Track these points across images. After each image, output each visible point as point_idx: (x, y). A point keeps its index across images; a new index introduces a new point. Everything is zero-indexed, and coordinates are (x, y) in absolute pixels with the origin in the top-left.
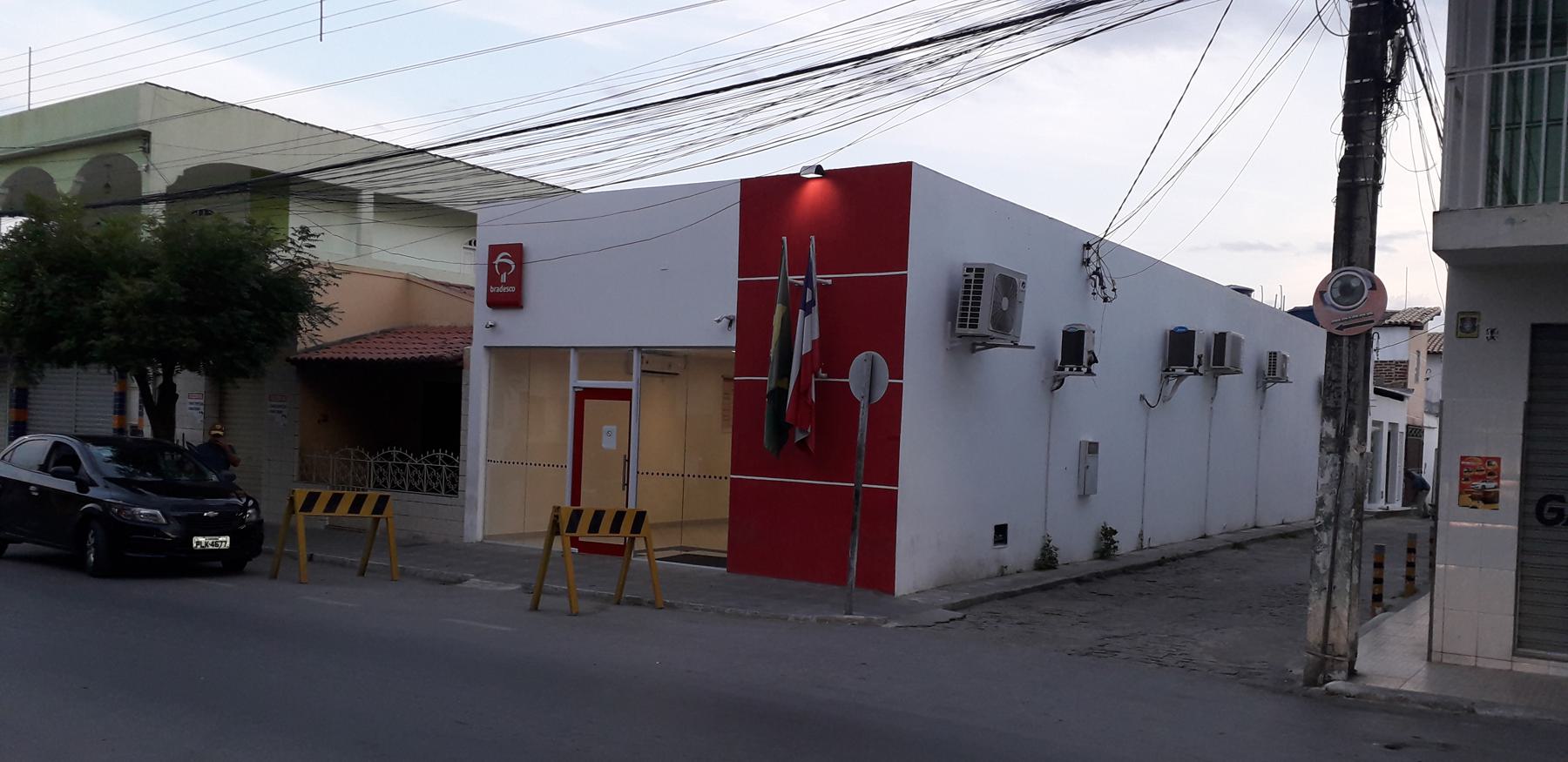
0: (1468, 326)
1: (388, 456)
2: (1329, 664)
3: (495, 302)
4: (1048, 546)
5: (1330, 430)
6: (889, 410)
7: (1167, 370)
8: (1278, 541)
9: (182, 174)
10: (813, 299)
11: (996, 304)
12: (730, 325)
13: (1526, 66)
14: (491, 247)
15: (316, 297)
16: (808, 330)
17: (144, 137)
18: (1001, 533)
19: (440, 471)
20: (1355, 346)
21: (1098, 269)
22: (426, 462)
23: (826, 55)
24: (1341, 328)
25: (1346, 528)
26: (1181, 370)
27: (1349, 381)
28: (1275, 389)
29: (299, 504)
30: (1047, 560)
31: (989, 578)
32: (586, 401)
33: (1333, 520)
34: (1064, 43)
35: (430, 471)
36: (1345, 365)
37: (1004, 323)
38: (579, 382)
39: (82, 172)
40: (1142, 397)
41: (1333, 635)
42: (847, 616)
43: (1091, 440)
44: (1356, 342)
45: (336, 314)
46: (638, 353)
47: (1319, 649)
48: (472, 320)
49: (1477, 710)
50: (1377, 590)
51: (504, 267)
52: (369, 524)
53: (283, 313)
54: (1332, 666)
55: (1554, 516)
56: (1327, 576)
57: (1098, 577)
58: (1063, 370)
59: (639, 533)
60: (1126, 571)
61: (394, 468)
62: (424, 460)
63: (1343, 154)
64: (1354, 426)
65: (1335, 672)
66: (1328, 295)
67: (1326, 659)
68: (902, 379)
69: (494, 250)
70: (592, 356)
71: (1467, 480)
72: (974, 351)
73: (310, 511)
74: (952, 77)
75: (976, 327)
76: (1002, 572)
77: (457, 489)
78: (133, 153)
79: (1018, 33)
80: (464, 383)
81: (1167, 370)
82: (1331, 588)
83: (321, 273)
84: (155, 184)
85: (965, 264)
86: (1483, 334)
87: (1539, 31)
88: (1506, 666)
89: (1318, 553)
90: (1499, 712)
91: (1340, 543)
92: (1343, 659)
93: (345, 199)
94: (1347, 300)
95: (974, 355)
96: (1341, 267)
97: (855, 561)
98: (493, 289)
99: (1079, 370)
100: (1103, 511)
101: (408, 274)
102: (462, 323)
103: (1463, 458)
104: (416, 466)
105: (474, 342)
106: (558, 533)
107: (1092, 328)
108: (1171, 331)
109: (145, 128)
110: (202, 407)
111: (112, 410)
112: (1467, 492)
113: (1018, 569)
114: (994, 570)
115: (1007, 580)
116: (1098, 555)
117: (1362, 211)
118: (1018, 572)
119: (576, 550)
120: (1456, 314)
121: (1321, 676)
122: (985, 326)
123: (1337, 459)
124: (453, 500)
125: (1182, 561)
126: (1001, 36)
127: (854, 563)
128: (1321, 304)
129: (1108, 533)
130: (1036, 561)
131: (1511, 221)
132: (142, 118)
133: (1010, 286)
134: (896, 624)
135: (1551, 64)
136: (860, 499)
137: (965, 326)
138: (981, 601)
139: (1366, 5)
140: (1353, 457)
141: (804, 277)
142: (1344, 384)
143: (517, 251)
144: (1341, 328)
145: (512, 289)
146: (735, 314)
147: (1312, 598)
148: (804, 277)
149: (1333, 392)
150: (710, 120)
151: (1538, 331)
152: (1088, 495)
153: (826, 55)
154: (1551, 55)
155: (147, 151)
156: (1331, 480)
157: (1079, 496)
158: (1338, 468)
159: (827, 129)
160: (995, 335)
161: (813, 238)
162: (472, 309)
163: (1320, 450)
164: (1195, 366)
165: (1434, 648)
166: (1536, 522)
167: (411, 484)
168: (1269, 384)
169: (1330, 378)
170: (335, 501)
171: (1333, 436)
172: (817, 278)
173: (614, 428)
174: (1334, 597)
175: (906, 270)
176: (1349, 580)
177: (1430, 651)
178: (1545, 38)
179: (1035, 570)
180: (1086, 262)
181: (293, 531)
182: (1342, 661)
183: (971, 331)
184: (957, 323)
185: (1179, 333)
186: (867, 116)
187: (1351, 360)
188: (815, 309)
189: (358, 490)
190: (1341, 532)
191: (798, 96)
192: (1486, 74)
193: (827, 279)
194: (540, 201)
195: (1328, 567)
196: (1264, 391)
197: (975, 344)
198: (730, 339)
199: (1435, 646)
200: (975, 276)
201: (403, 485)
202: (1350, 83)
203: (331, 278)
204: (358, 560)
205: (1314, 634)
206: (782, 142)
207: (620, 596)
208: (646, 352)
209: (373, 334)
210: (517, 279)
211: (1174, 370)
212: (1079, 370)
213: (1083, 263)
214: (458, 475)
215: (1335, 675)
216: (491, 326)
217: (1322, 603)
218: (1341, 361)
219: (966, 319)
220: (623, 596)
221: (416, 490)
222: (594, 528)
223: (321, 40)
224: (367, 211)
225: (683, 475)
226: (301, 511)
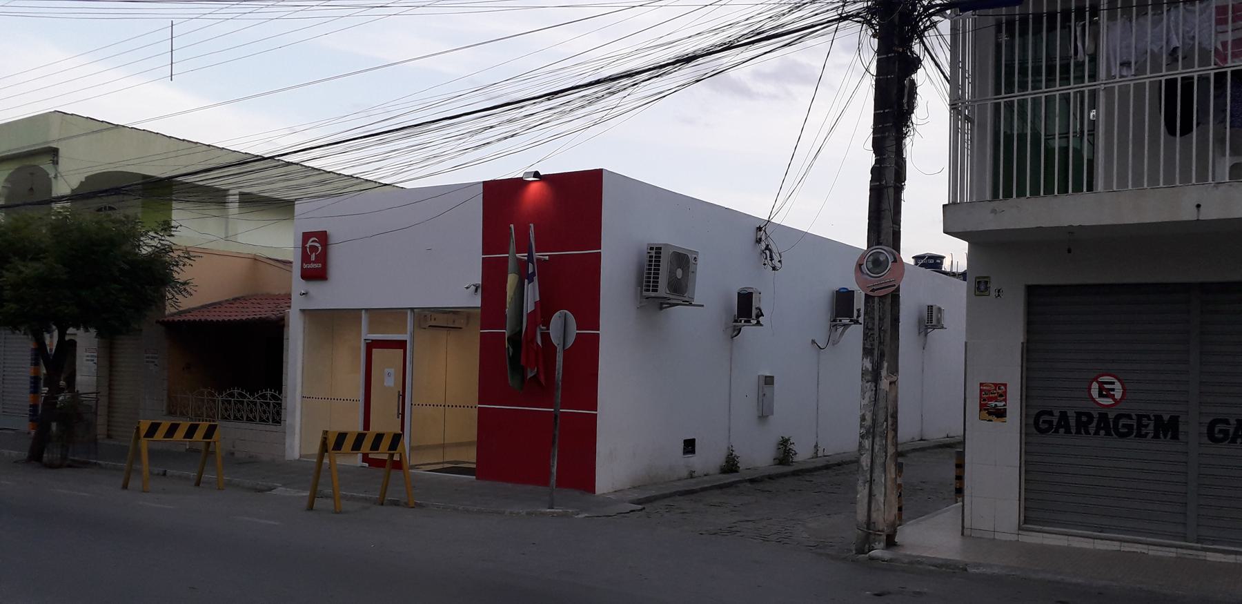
0: (982, 287)
1: (232, 395)
2: (872, 537)
3: (307, 275)
4: (732, 454)
5: (869, 366)
6: (587, 351)
7: (834, 321)
8: (936, 450)
9: (84, 180)
10: (534, 272)
11: (672, 273)
12: (476, 290)
13: (1030, 94)
14: (304, 234)
15: (175, 275)
16: (532, 293)
17: (53, 153)
18: (690, 446)
19: (268, 405)
20: (884, 303)
21: (768, 245)
22: (259, 399)
23: (528, 91)
24: (873, 290)
25: (881, 436)
26: (846, 321)
27: (880, 329)
28: (935, 334)
29: (143, 433)
30: (731, 466)
31: (680, 480)
32: (373, 350)
33: (872, 431)
34: (689, 84)
35: (261, 405)
36: (877, 318)
37: (680, 289)
38: (369, 335)
39: (7, 180)
40: (813, 342)
41: (874, 515)
42: (548, 510)
43: (768, 375)
44: (884, 301)
45: (192, 287)
46: (411, 312)
47: (865, 526)
48: (290, 287)
49: (968, 569)
50: (958, 484)
51: (313, 249)
52: (202, 447)
53: (147, 287)
54: (874, 539)
55: (1046, 426)
56: (869, 471)
57: (770, 478)
58: (741, 321)
59: (396, 450)
60: (795, 473)
61: (235, 404)
62: (257, 397)
63: (874, 163)
64: (884, 362)
65: (877, 543)
66: (864, 267)
67: (870, 533)
68: (599, 330)
69: (306, 236)
70: (380, 316)
71: (985, 400)
72: (661, 308)
73: (153, 437)
74: (613, 108)
75: (656, 291)
76: (691, 475)
77: (280, 419)
78: (45, 164)
79: (657, 77)
80: (285, 337)
81: (834, 321)
82: (871, 482)
83: (179, 256)
84: (62, 188)
85: (648, 244)
86: (993, 294)
87: (1037, 71)
88: (1014, 538)
89: (862, 455)
90: (982, 570)
91: (877, 448)
92: (882, 533)
93: (216, 197)
94: (877, 270)
95: (662, 311)
96: (873, 246)
97: (555, 467)
98: (305, 266)
99: (749, 322)
100: (779, 427)
101: (255, 255)
102: (283, 292)
103: (981, 384)
104: (251, 402)
105: (293, 305)
106: (327, 451)
107: (760, 290)
108: (837, 291)
109: (54, 145)
110: (96, 359)
111: (30, 361)
112: (985, 410)
113: (705, 473)
114: (685, 473)
115: (693, 481)
116: (777, 461)
117: (887, 205)
118: (705, 475)
119: (367, 465)
120: (974, 280)
121: (867, 546)
122: (663, 290)
123: (873, 384)
124: (278, 428)
125: (845, 466)
126: (647, 78)
127: (554, 470)
128: (860, 273)
129: (784, 442)
130: (721, 466)
131: (994, 211)
132: (51, 137)
133: (683, 260)
134: (587, 515)
135: (1046, 94)
136: (558, 421)
137: (648, 290)
138: (664, 496)
139: (885, 56)
140: (884, 384)
141: (526, 254)
142: (876, 328)
143: (323, 237)
144: (873, 290)
145: (320, 265)
146: (480, 283)
147: (859, 488)
148: (526, 254)
149: (870, 337)
150: (448, 138)
151: (1031, 291)
152: (768, 416)
153: (528, 91)
154: (1046, 88)
155: (56, 163)
156: (870, 402)
157: (759, 417)
158: (873, 392)
159: (531, 145)
160: (671, 296)
161: (532, 225)
162: (291, 278)
163: (862, 380)
164: (855, 317)
165: (965, 526)
166: (1035, 431)
167: (235, 415)
168: (929, 330)
169: (867, 328)
170: (173, 429)
171: (870, 369)
172: (537, 255)
173: (392, 371)
174: (874, 487)
175: (600, 249)
176: (883, 475)
177: (963, 527)
178: (1041, 75)
179: (720, 473)
180: (759, 241)
181: (137, 453)
182: (881, 535)
183: (653, 294)
184: (644, 288)
185: (843, 292)
186: (557, 136)
187: (881, 314)
188: (536, 279)
189: (210, 421)
190: (877, 439)
191: (510, 121)
192: (989, 103)
193: (545, 256)
194: (336, 199)
195: (869, 465)
196: (926, 335)
197: (662, 304)
198: (477, 302)
199: (967, 524)
200: (656, 252)
201: (242, 417)
202: (878, 112)
203: (186, 260)
204: (193, 474)
205: (861, 515)
206: (498, 156)
207: (384, 497)
208: (433, 311)
209: (227, 301)
210: (323, 258)
211: (840, 321)
212: (749, 322)
213: (757, 241)
214: (281, 408)
215: (877, 545)
216: (304, 294)
217: (866, 491)
218: (874, 314)
219: (653, 287)
220: (386, 498)
221: (238, 419)
222: (375, 446)
223: (171, 80)
224: (233, 208)
225: (444, 406)
226: (144, 437)
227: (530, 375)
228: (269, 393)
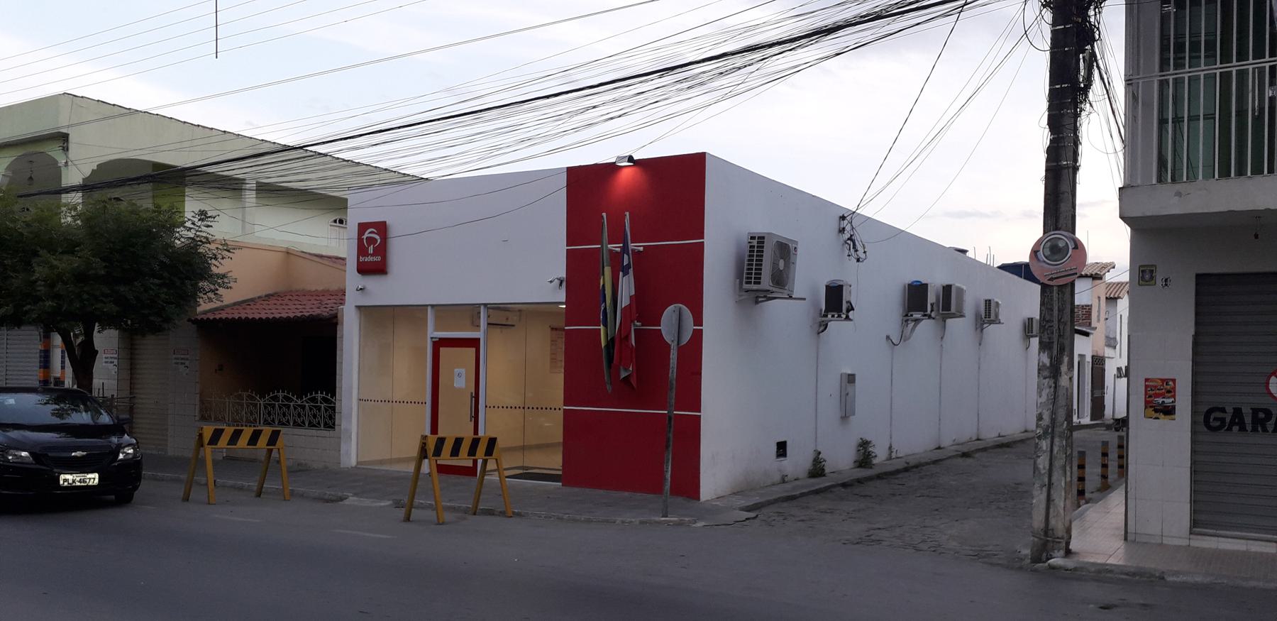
0: (1147, 277)
1: (275, 398)
3: (364, 270)
5: (1046, 361)
6: (692, 351)
7: (907, 315)
9: (95, 168)
11: (775, 264)
16: (627, 287)
17: (62, 139)
18: (782, 448)
19: (319, 409)
20: (1063, 293)
21: (851, 236)
22: (308, 403)
24: (1051, 279)
25: (1060, 436)
26: (917, 315)
27: (1059, 321)
28: (991, 329)
29: (207, 438)
31: (773, 485)
32: (441, 349)
34: (828, 58)
36: (1056, 308)
37: (781, 280)
38: (436, 333)
39: (8, 168)
40: (888, 337)
41: (1053, 522)
43: (850, 372)
49: (1165, 577)
52: (262, 455)
54: (1053, 546)
56: (1047, 475)
58: (827, 316)
60: (880, 477)
61: (280, 408)
62: (305, 401)
65: (1056, 551)
66: (1041, 254)
69: (363, 227)
70: (446, 312)
71: (1150, 396)
72: (757, 302)
75: (759, 283)
76: (783, 480)
77: (334, 424)
78: (54, 151)
79: (791, 50)
81: (907, 315)
82: (1050, 485)
83: (217, 248)
84: (72, 176)
86: (1159, 282)
87: (1195, 47)
88: (1184, 542)
91: (1056, 449)
93: (232, 186)
94: (1056, 257)
96: (1050, 231)
97: (670, 473)
98: (362, 259)
99: (839, 316)
100: (863, 425)
101: (287, 248)
102: (334, 287)
103: (1147, 380)
104: (299, 405)
106: (426, 457)
107: (849, 283)
108: (909, 285)
109: (64, 131)
110: (116, 361)
111: (38, 364)
112: (1151, 407)
113: (795, 477)
114: (777, 478)
115: (788, 486)
117: (1065, 187)
121: (1045, 554)
122: (766, 282)
123: (1051, 382)
126: (777, 52)
127: (668, 475)
129: (864, 444)
130: (809, 470)
131: (1179, 194)
132: (61, 123)
133: (785, 250)
134: (703, 524)
136: (672, 423)
137: (750, 283)
138: (769, 503)
139: (1063, 27)
141: (621, 245)
142: (1055, 319)
143: (382, 228)
144: (1051, 279)
145: (378, 259)
146: (565, 276)
147: (1036, 493)
148: (621, 245)
151: (1201, 279)
152: (848, 417)
155: (66, 149)
156: (1048, 400)
157: (842, 418)
158: (1052, 390)
160: (774, 289)
163: (1038, 376)
164: (929, 312)
165: (1129, 531)
167: (295, 420)
168: (985, 325)
171: (1048, 365)
172: (632, 246)
173: (463, 371)
174: (1052, 492)
176: (1063, 478)
177: (1126, 532)
179: (810, 477)
180: (842, 230)
181: (201, 462)
182: (1059, 542)
183: (755, 287)
185: (916, 286)
187: (1060, 304)
188: (631, 271)
190: (1057, 440)
191: (615, 100)
193: (639, 246)
195: (1048, 468)
196: (982, 330)
197: (757, 297)
198: (561, 296)
199: (1131, 529)
200: (757, 243)
204: (254, 485)
205: (1038, 520)
206: (601, 138)
207: (477, 507)
209: (259, 297)
210: (382, 250)
211: (912, 315)
212: (839, 316)
213: (840, 231)
215: (1056, 553)
216: (361, 289)
217: (1043, 497)
218: (1052, 305)
220: (479, 508)
222: (455, 452)
223: (217, 57)
224: (250, 197)
225: (524, 408)
226: (208, 444)
227: (623, 374)
228: (319, 396)
